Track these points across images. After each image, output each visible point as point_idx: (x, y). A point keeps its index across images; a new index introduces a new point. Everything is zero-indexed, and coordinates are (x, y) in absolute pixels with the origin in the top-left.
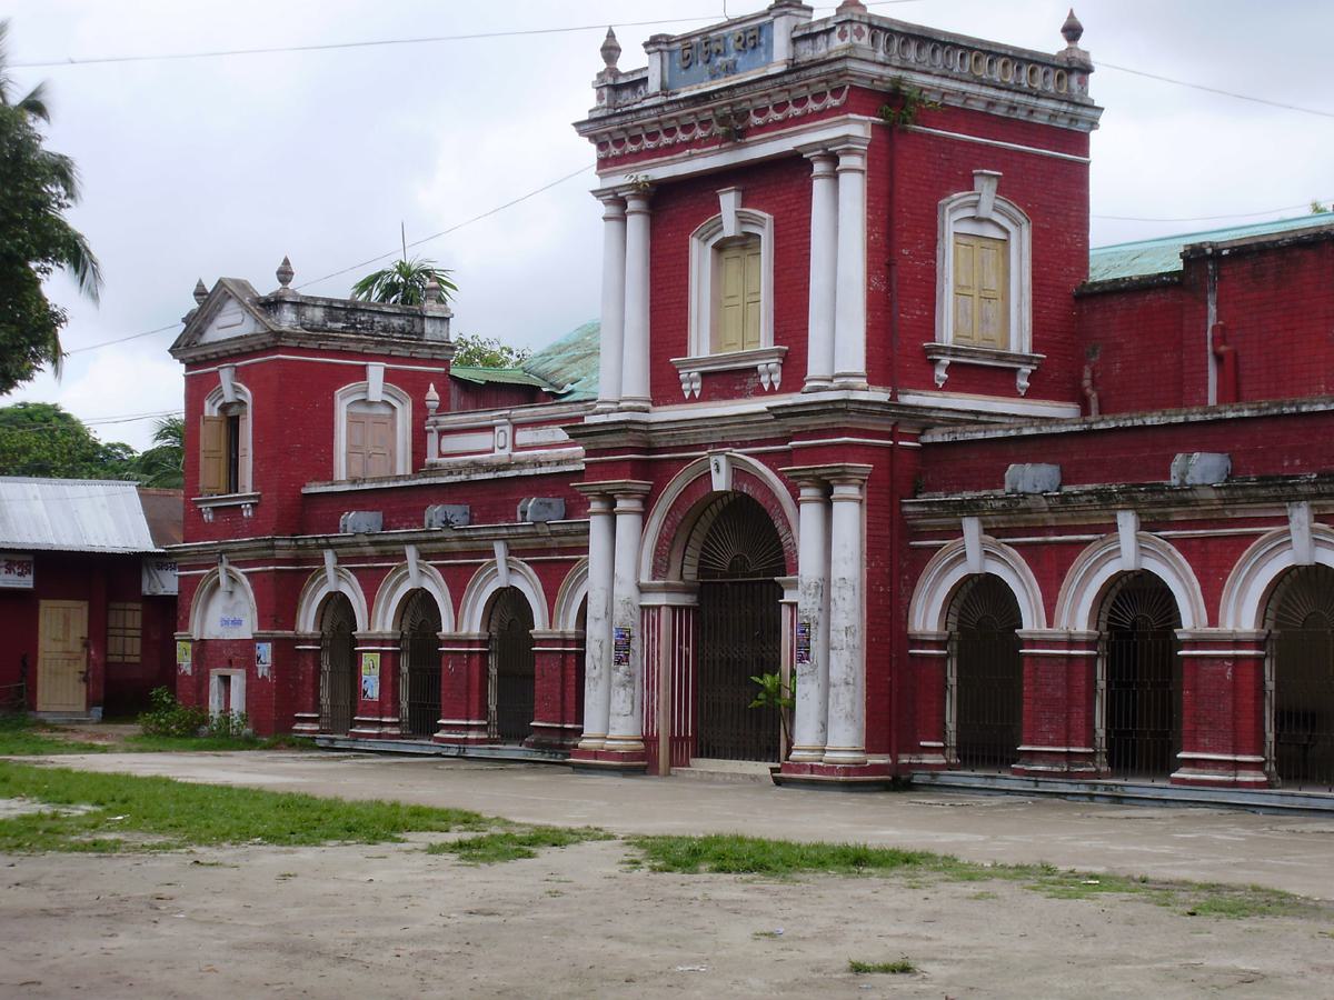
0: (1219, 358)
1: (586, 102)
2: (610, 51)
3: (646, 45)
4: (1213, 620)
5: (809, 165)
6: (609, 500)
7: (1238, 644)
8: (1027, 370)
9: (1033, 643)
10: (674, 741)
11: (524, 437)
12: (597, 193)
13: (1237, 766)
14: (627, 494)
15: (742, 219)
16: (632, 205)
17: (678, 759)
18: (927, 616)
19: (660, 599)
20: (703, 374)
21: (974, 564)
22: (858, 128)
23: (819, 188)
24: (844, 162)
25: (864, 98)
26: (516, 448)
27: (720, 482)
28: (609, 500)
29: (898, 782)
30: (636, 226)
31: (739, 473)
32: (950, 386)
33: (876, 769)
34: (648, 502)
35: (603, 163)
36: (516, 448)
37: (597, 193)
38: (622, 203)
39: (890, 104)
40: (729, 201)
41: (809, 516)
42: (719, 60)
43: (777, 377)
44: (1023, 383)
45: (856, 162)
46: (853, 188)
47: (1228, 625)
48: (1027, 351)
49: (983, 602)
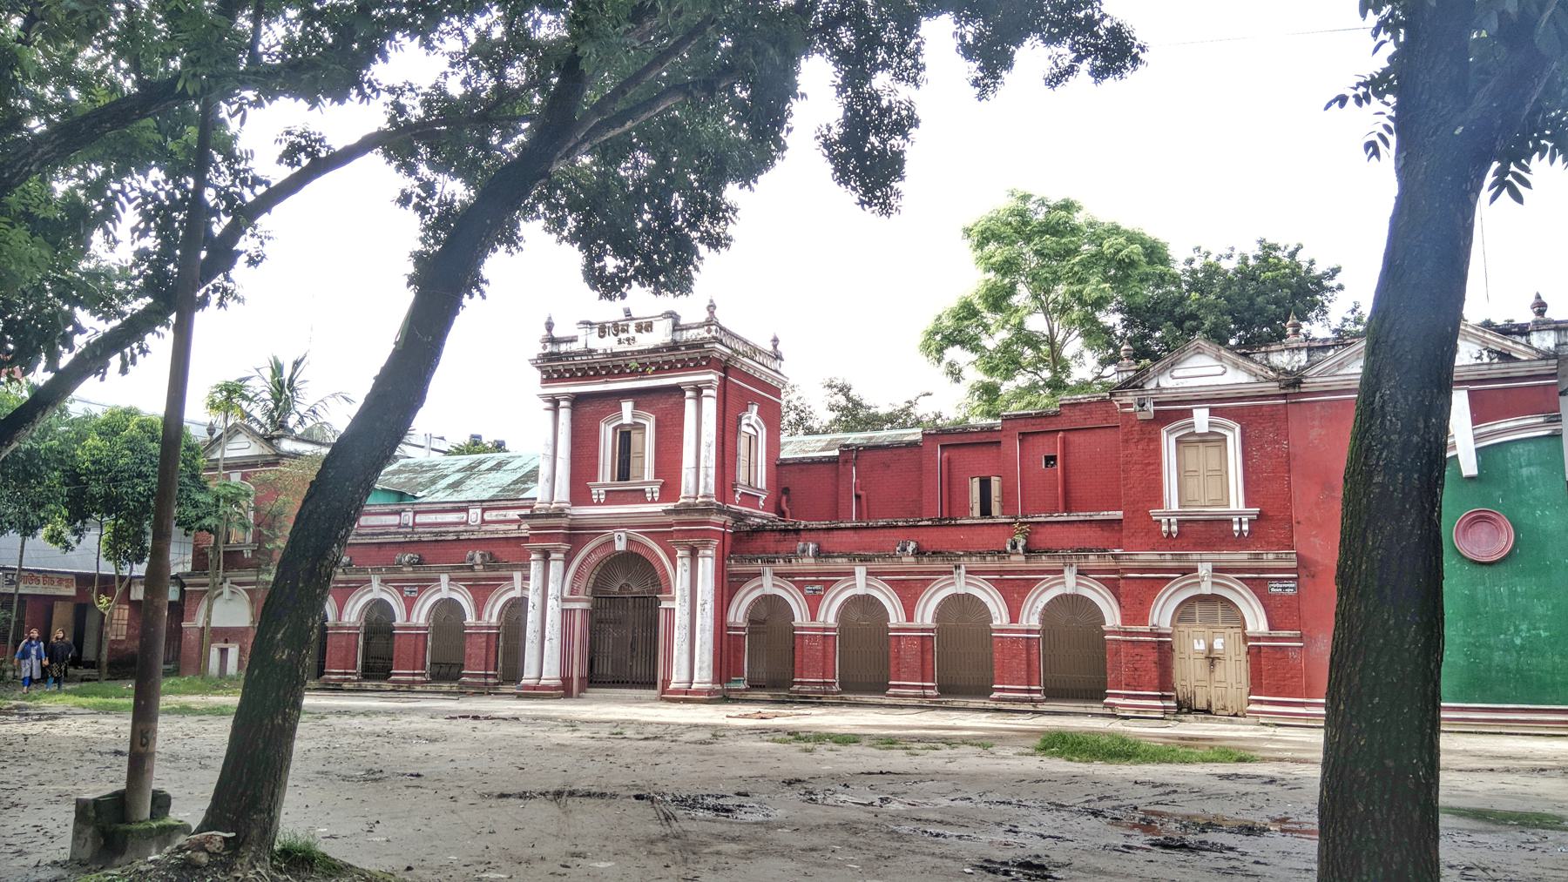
0: (858, 497)
1: (537, 349)
2: (550, 326)
4: (910, 618)
5: (683, 392)
6: (546, 556)
7: (923, 630)
9: (802, 629)
10: (580, 679)
12: (542, 396)
13: (923, 687)
14: (557, 551)
15: (634, 416)
16: (562, 403)
17: (582, 689)
18: (738, 614)
19: (577, 606)
22: (713, 376)
23: (690, 405)
24: (705, 392)
25: (710, 362)
27: (620, 546)
28: (546, 556)
29: (725, 699)
30: (565, 415)
31: (630, 541)
33: (716, 692)
35: (544, 381)
37: (542, 396)
39: (725, 367)
40: (627, 407)
41: (683, 564)
42: (623, 336)
43: (656, 495)
45: (713, 393)
46: (710, 406)
47: (917, 622)
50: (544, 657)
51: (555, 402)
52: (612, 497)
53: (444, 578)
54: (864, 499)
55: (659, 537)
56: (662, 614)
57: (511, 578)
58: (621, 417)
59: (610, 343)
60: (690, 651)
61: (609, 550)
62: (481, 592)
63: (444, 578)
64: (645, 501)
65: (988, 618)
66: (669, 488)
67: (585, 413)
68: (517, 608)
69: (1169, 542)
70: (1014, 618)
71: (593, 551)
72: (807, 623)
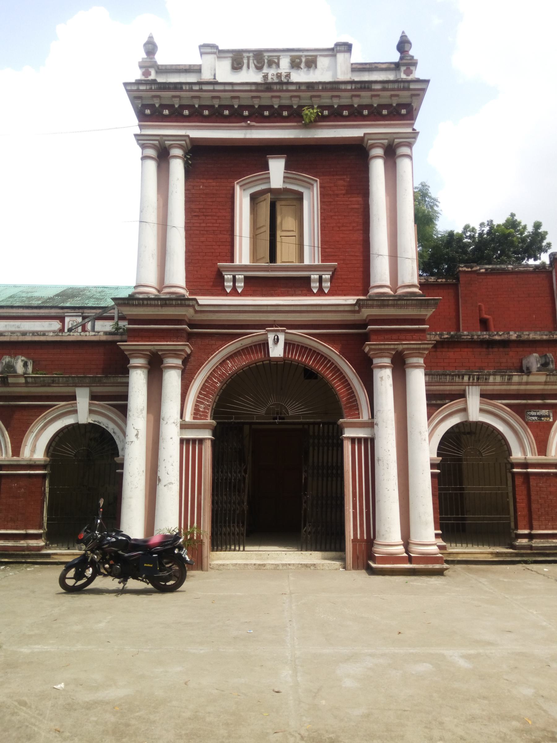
2: (151, 48)
3: (201, 47)
14: (175, 354)
27: (277, 351)
30: (177, 168)
40: (277, 167)
43: (327, 285)
51: (163, 156)
57: (73, 398)
58: (268, 179)
60: (402, 498)
61: (257, 357)
64: (310, 293)
65: (509, 452)
67: (213, 170)
71: (231, 357)
72: (532, 457)
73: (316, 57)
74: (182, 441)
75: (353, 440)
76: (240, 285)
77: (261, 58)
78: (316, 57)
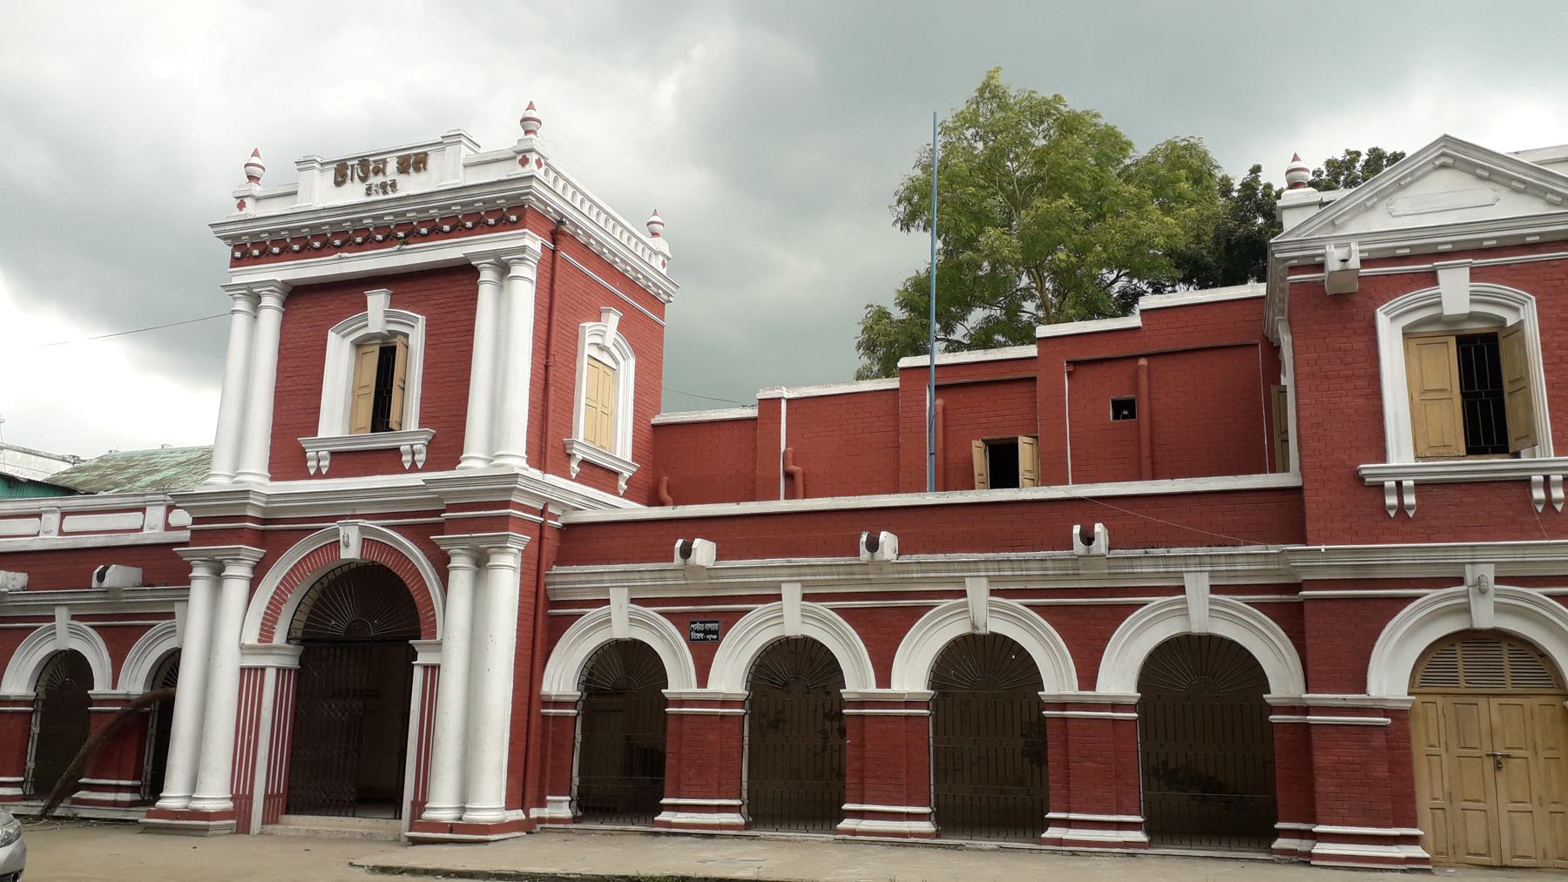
8: (627, 475)
9: (681, 703)
11: (71, 523)
18: (562, 677)
20: (333, 453)
21: (621, 630)
26: (61, 532)
27: (351, 551)
32: (580, 479)
34: (259, 572)
35: (236, 262)
36: (61, 532)
38: (258, 298)
40: (377, 301)
42: (375, 180)
43: (421, 458)
44: (622, 485)
46: (524, 292)
48: (628, 458)
49: (626, 668)
50: (208, 756)
52: (346, 461)
53: (62, 615)
54: (799, 480)
55: (420, 534)
56: (418, 675)
59: (354, 193)
62: (120, 639)
63: (62, 615)
66: (447, 445)
68: (168, 670)
69: (1402, 525)
70: (1088, 678)
73: (426, 154)
74: (242, 669)
75: (426, 667)
76: (325, 463)
77: (367, 167)
78: (426, 154)
